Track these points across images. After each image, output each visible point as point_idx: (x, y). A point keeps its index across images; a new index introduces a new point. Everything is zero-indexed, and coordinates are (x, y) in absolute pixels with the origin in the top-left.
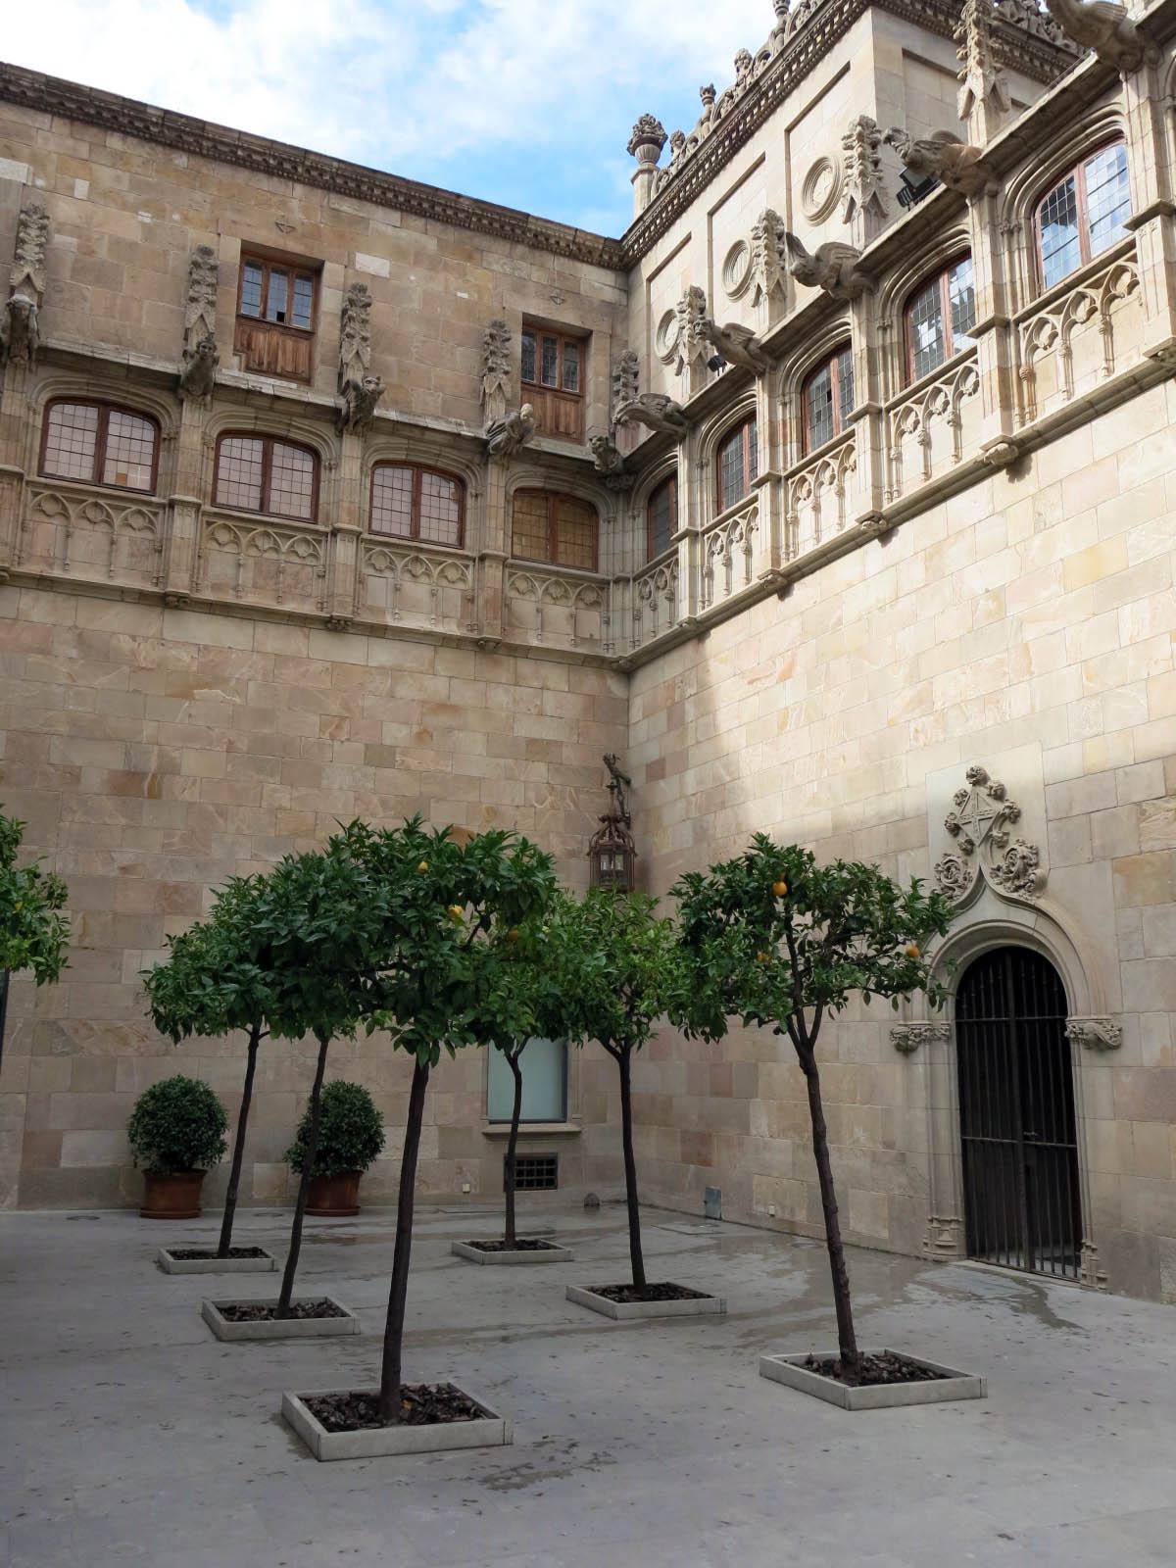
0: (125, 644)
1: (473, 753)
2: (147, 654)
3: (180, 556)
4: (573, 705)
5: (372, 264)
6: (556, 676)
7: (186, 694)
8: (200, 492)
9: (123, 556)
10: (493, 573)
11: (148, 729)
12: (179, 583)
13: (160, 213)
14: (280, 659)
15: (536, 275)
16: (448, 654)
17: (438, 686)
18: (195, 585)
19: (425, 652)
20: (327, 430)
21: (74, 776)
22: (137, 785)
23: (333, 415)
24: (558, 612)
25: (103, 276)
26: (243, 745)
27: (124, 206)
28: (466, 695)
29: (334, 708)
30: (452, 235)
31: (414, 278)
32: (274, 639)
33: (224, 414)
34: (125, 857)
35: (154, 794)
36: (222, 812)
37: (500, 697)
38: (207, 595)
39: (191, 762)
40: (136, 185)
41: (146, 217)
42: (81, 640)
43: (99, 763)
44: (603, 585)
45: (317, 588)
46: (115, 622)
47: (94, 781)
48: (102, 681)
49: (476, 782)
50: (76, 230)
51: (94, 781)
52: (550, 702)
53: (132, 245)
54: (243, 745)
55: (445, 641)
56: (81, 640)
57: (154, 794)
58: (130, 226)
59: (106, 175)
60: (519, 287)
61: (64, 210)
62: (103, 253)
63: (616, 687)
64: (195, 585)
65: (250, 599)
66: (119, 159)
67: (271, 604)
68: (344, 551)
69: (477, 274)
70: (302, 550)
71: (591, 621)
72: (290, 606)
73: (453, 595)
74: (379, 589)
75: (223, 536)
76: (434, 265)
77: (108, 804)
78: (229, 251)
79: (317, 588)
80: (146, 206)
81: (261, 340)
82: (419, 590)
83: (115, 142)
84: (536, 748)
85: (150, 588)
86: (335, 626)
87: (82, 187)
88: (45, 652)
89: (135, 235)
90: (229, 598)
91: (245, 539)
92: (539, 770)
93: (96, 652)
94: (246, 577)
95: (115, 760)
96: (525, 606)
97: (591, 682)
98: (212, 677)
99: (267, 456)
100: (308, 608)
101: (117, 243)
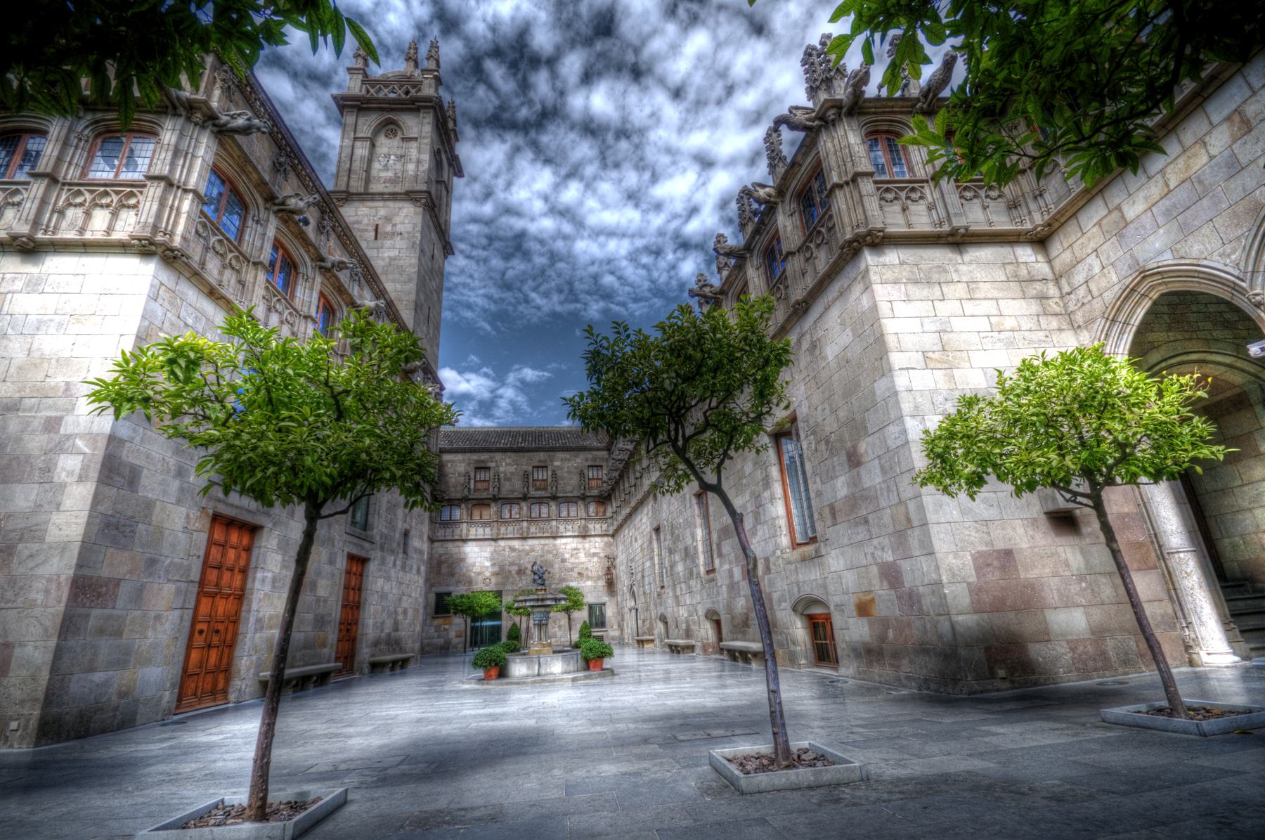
1: (582, 557)
4: (602, 545)
5: (557, 463)
6: (598, 539)
17: (574, 545)
24: (598, 526)
28: (580, 546)
31: (566, 464)
32: (543, 541)
37: (587, 545)
43: (515, 568)
58: (512, 469)
61: (502, 469)
69: (579, 460)
73: (576, 527)
74: (562, 528)
76: (569, 460)
78: (530, 469)
82: (570, 527)
84: (595, 555)
92: (596, 559)
93: (512, 549)
96: (591, 526)
97: (606, 539)
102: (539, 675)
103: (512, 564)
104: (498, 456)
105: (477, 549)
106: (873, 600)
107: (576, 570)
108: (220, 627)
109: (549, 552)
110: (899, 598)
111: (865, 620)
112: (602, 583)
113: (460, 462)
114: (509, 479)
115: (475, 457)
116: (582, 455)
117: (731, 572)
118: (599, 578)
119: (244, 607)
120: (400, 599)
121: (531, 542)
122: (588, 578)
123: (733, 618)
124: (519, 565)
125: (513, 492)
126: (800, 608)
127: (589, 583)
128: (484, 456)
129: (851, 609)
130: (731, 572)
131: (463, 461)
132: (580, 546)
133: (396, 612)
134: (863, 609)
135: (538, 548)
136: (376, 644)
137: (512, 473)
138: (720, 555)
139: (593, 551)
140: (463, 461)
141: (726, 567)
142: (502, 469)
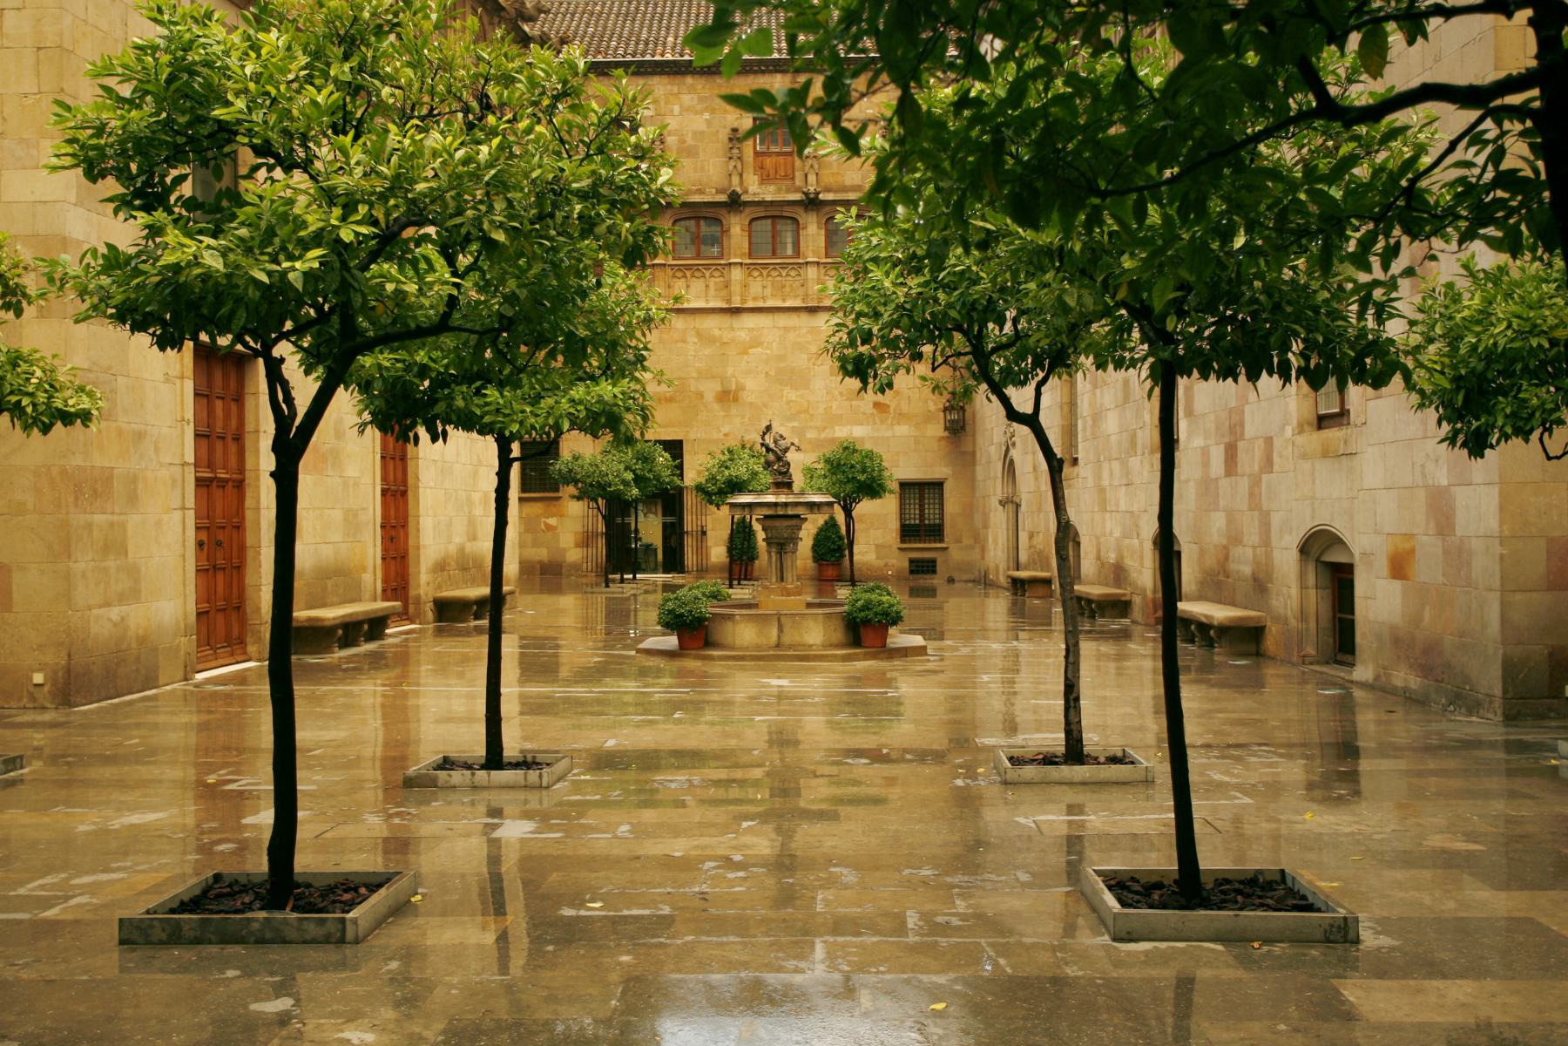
0: (717, 332)
2: (727, 336)
3: (736, 288)
7: (745, 352)
8: (742, 255)
9: (712, 292)
11: (730, 371)
12: (736, 303)
14: (786, 329)
18: (744, 301)
20: (800, 210)
21: (701, 395)
22: (728, 397)
25: (691, 152)
26: (772, 373)
27: (697, 113)
32: (783, 320)
33: (748, 214)
34: (726, 429)
35: (736, 400)
36: (765, 406)
38: (750, 304)
40: (701, 100)
41: (707, 116)
42: (698, 334)
43: (710, 389)
45: (801, 291)
46: (711, 323)
47: (710, 397)
48: (708, 351)
50: (676, 132)
53: (702, 133)
54: (772, 373)
58: (699, 122)
59: (687, 99)
61: (673, 123)
62: (690, 141)
64: (744, 301)
65: (770, 303)
66: (692, 90)
67: (779, 304)
68: (812, 272)
70: (793, 273)
72: (787, 304)
75: (756, 273)
77: (716, 406)
79: (801, 291)
80: (706, 109)
81: (768, 161)
83: (689, 80)
85: (725, 306)
86: (812, 310)
87: (676, 109)
88: (684, 341)
89: (702, 127)
90: (760, 304)
91: (765, 272)
93: (705, 338)
94: (768, 291)
98: (756, 342)
99: (773, 225)
100: (798, 303)
101: (695, 133)
102: (778, 646)
106: (1412, 551)
108: (221, 536)
110: (1446, 552)
111: (1397, 584)
112: (937, 429)
117: (1205, 452)
118: (928, 418)
119: (249, 502)
120: (476, 473)
121: (749, 321)
123: (1202, 552)
124: (723, 379)
126: (1315, 551)
127: (903, 430)
129: (1382, 565)
130: (1205, 452)
133: (469, 499)
134: (1399, 568)
136: (440, 567)
137: (698, 135)
138: (1189, 413)
141: (1198, 442)
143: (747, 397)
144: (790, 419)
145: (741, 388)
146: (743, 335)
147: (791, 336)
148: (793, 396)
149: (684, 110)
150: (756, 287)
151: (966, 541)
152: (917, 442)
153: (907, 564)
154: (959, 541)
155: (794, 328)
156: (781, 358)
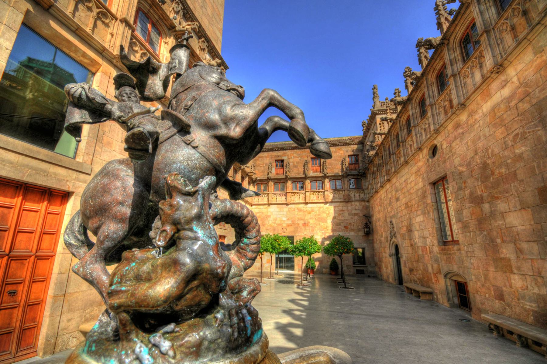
2: (305, 209)
4: (361, 208)
7: (310, 213)
10: (346, 192)
12: (307, 201)
13: (301, 157)
14: (320, 207)
15: (350, 149)
16: (342, 203)
19: (339, 204)
22: (306, 225)
23: (323, 176)
24: (357, 195)
29: (327, 213)
30: (337, 147)
34: (305, 233)
35: (307, 225)
39: (311, 221)
43: (301, 223)
44: (363, 190)
47: (301, 225)
48: (301, 213)
49: (347, 220)
51: (301, 225)
52: (357, 208)
55: (341, 202)
56: (298, 209)
57: (307, 225)
58: (298, 160)
59: (295, 155)
60: (347, 151)
62: (296, 164)
63: (367, 204)
66: (296, 153)
69: (342, 152)
71: (362, 195)
83: (295, 151)
84: (356, 214)
92: (356, 217)
93: (300, 210)
95: (302, 222)
96: (352, 195)
97: (363, 204)
98: (313, 211)
100: (323, 201)
103: (300, 219)
104: (289, 152)
105: (278, 210)
107: (343, 225)
109: (324, 212)
112: (361, 234)
113: (266, 157)
114: (295, 166)
115: (275, 153)
116: (344, 148)
118: (359, 230)
122: (352, 230)
124: (304, 220)
125: (298, 174)
127: (352, 233)
128: (280, 153)
131: (268, 156)
132: (345, 208)
135: (316, 209)
139: (354, 212)
140: (268, 156)
142: (291, 160)
143: (310, 225)
144: (322, 230)
145: (309, 222)
146: (309, 209)
147: (321, 209)
148: (322, 224)
149: (294, 157)
150: (312, 197)
151: (373, 265)
152: (356, 237)
153: (355, 271)
154: (370, 265)
155: (322, 207)
156: (319, 215)
